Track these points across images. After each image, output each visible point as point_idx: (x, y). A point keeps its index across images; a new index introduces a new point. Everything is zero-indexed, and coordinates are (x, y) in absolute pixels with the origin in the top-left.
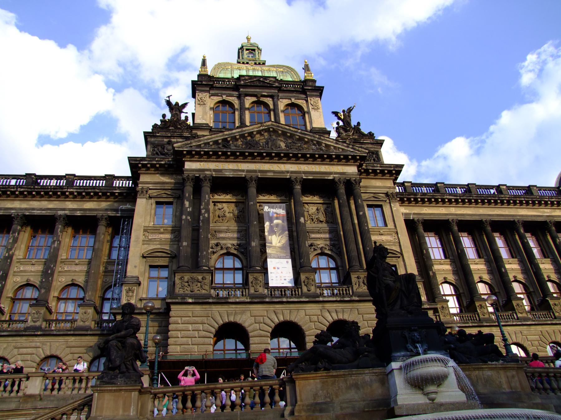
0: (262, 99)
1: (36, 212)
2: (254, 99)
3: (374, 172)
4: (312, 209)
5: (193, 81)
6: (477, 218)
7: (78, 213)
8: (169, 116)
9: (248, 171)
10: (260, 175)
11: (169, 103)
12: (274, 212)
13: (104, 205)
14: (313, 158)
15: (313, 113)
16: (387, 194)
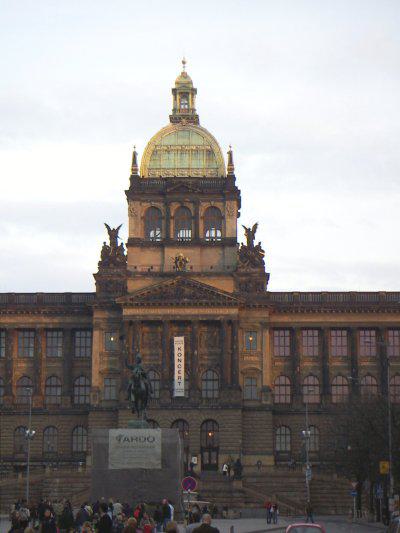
0: (187, 205)
1: (22, 326)
2: (179, 205)
3: (254, 306)
4: (205, 337)
5: (126, 191)
6: (346, 325)
7: (51, 326)
8: (108, 244)
9: (164, 315)
10: (171, 318)
11: (107, 226)
12: (179, 343)
13: (69, 320)
14: (207, 305)
15: (228, 220)
16: (261, 323)
